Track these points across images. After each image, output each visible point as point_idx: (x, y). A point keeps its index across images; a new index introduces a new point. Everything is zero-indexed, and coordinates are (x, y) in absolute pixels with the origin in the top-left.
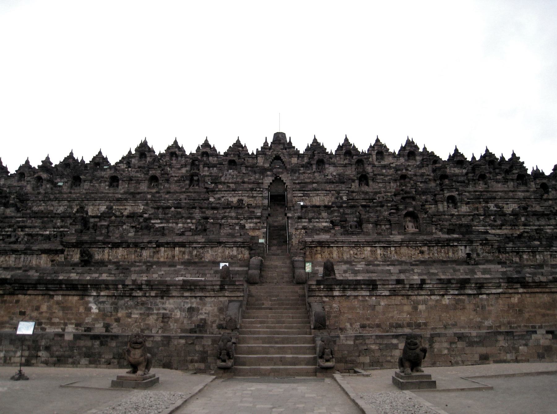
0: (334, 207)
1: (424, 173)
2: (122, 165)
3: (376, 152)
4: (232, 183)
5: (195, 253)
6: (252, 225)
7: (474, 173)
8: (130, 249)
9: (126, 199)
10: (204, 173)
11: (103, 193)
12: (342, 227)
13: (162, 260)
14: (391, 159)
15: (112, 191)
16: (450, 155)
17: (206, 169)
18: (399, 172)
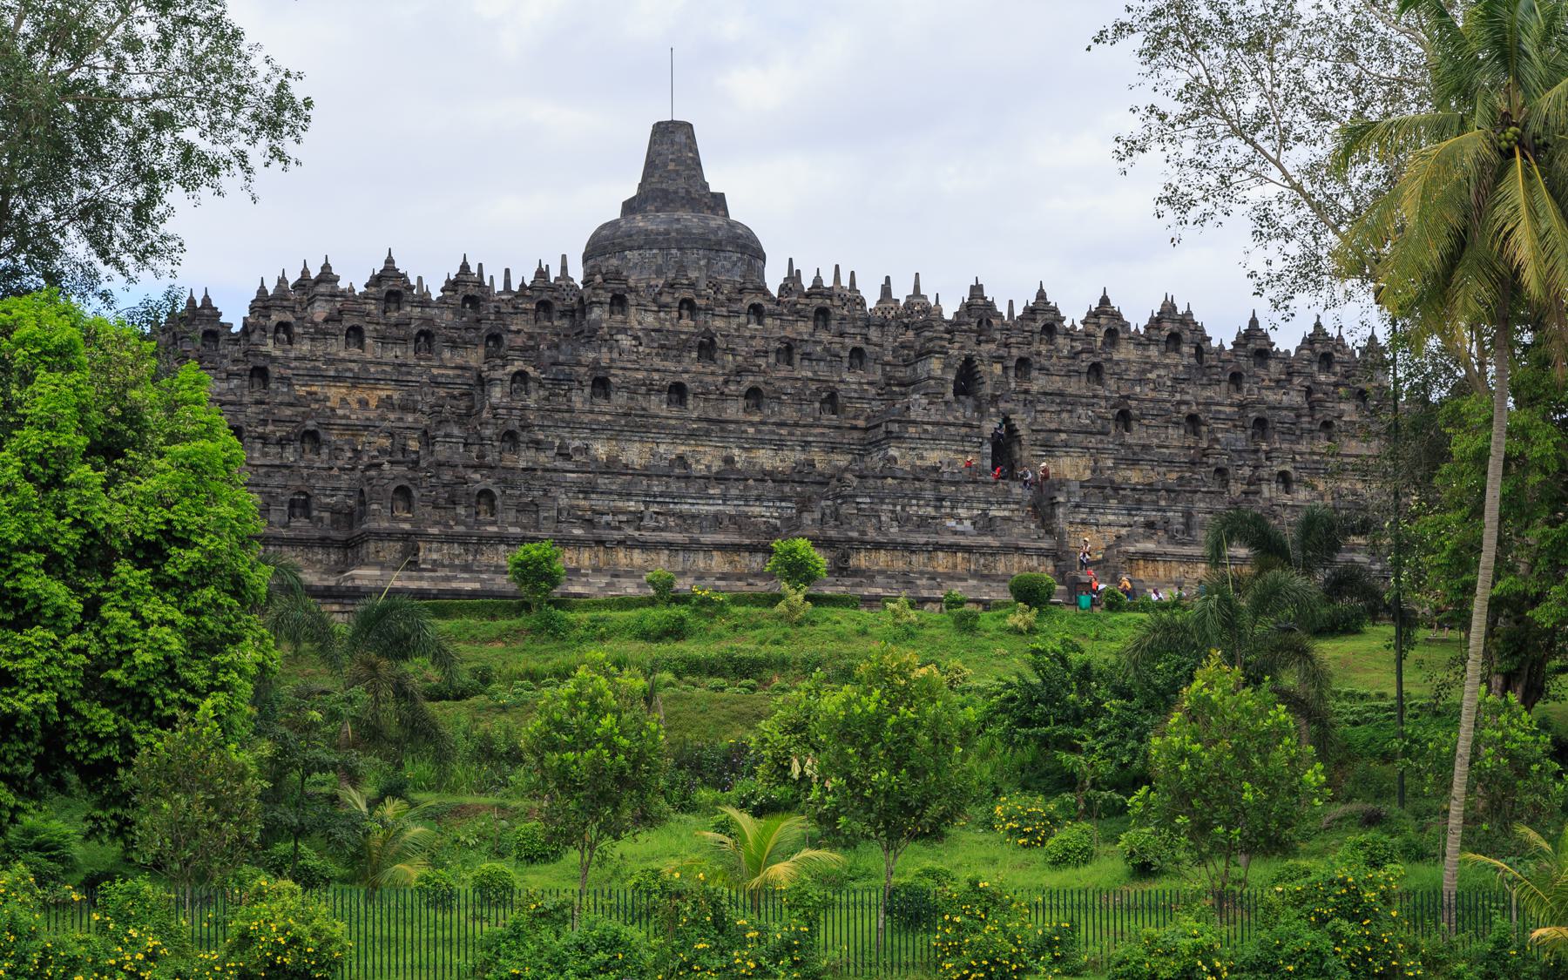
0: (1124, 489)
1: (1211, 397)
2: (623, 337)
3: (1104, 330)
4: (928, 423)
5: (982, 561)
6: (1006, 513)
7: (1312, 416)
8: (896, 553)
9: (708, 433)
10: (804, 373)
11: (657, 417)
12: (1166, 531)
13: (940, 570)
14: (1132, 346)
15: (675, 414)
16: (1240, 333)
17: (806, 363)
18: (1184, 408)
